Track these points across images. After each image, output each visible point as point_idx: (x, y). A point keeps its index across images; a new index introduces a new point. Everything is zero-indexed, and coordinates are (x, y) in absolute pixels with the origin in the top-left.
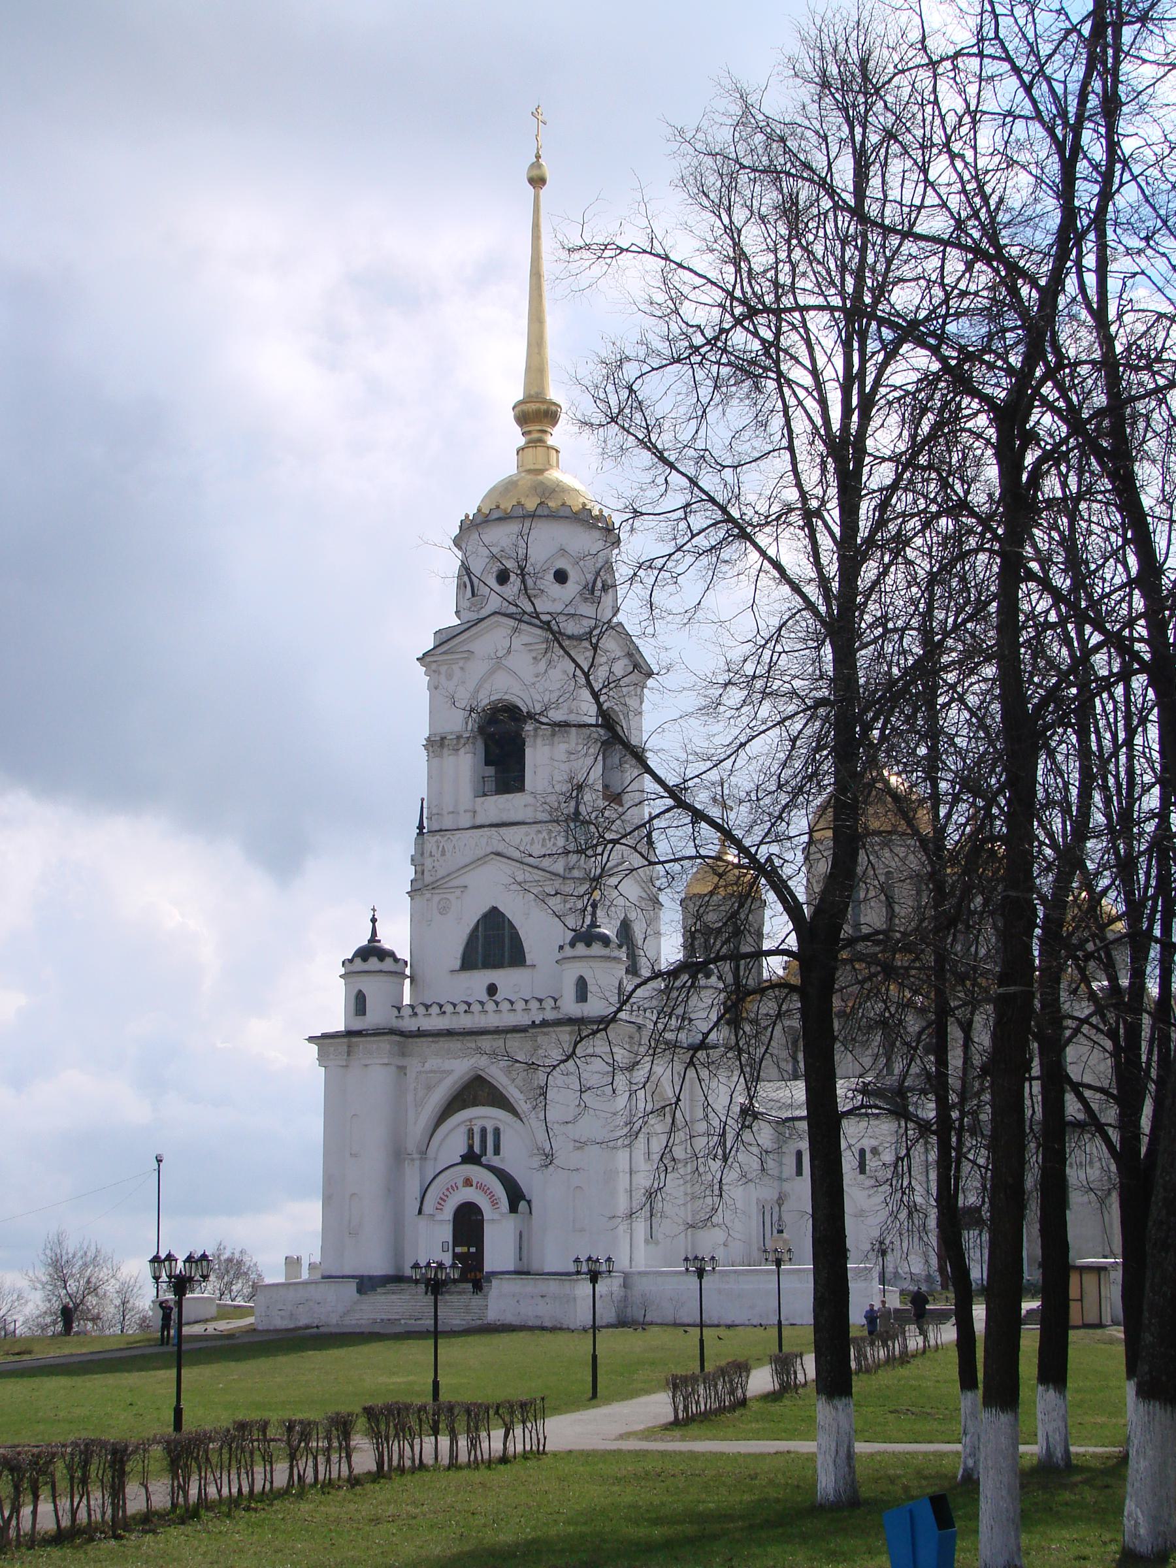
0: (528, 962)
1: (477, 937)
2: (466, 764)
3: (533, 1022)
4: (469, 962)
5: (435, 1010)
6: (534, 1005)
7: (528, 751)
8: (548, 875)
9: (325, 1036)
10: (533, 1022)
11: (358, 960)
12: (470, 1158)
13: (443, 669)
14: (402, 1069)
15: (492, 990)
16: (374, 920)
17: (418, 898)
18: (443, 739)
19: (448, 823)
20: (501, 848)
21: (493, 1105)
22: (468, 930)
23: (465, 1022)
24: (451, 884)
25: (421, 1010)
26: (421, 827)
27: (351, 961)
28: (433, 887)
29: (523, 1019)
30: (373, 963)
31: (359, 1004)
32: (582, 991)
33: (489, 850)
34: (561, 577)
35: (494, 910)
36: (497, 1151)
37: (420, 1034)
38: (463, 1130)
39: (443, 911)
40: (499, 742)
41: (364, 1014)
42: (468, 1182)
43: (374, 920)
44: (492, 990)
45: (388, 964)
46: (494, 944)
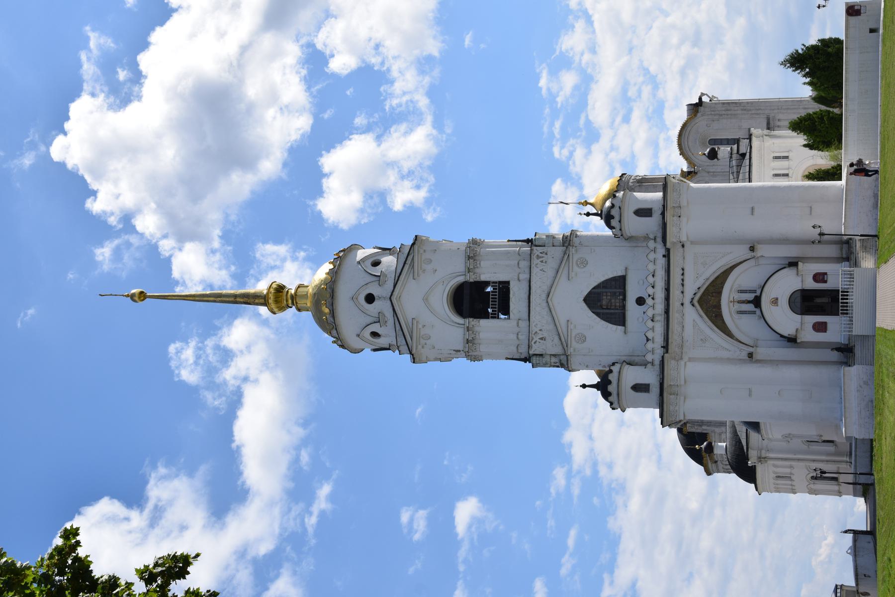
0: (623, 273)
1: (603, 314)
2: (486, 327)
3: (664, 256)
4: (618, 318)
5: (650, 335)
6: (652, 256)
7: (484, 278)
8: (566, 257)
9: (661, 416)
10: (664, 256)
11: (610, 398)
12: (757, 302)
13: (423, 341)
14: (690, 360)
15: (640, 301)
16: (584, 386)
17: (573, 361)
18: (468, 341)
19: (523, 337)
20: (544, 296)
21: (719, 293)
22: (598, 319)
23: (660, 307)
24: (565, 333)
25: (650, 345)
26: (525, 360)
27: (611, 404)
28: (565, 345)
29: (662, 261)
30: (613, 377)
31: (640, 388)
32: (643, 212)
33: (545, 304)
34: (376, 264)
35: (585, 300)
36: (755, 291)
37: (666, 347)
38: (736, 316)
39: (582, 339)
40: (477, 300)
41: (648, 385)
42: (775, 301)
43: (584, 386)
44: (640, 301)
45: (615, 369)
46: (607, 301)
